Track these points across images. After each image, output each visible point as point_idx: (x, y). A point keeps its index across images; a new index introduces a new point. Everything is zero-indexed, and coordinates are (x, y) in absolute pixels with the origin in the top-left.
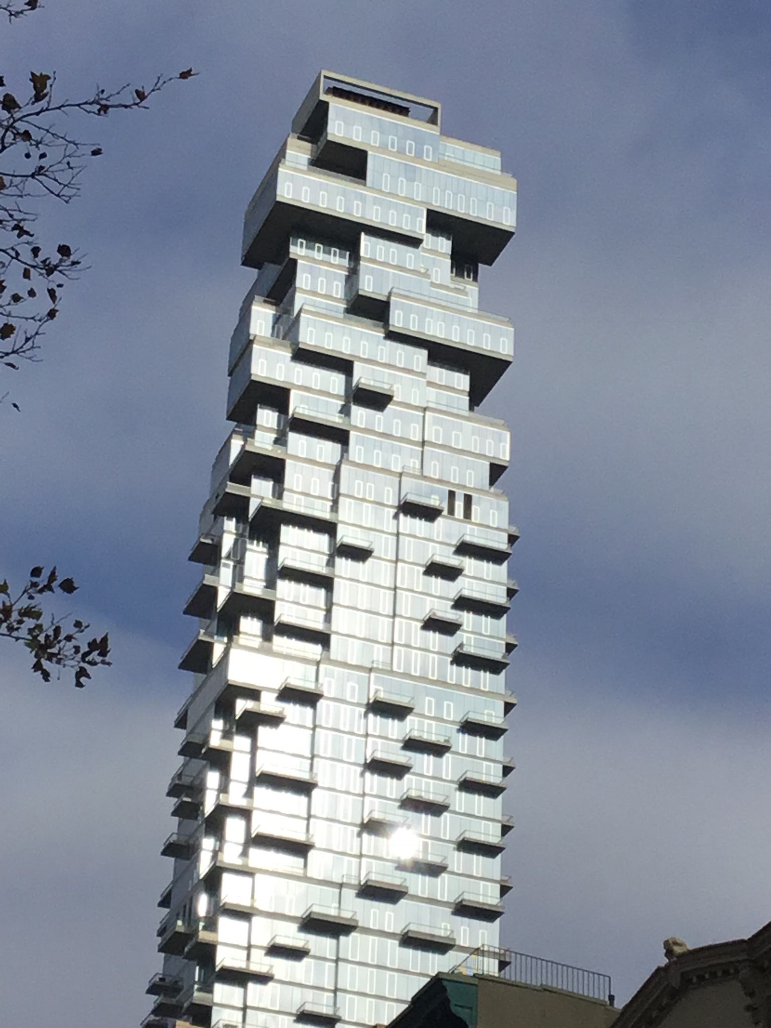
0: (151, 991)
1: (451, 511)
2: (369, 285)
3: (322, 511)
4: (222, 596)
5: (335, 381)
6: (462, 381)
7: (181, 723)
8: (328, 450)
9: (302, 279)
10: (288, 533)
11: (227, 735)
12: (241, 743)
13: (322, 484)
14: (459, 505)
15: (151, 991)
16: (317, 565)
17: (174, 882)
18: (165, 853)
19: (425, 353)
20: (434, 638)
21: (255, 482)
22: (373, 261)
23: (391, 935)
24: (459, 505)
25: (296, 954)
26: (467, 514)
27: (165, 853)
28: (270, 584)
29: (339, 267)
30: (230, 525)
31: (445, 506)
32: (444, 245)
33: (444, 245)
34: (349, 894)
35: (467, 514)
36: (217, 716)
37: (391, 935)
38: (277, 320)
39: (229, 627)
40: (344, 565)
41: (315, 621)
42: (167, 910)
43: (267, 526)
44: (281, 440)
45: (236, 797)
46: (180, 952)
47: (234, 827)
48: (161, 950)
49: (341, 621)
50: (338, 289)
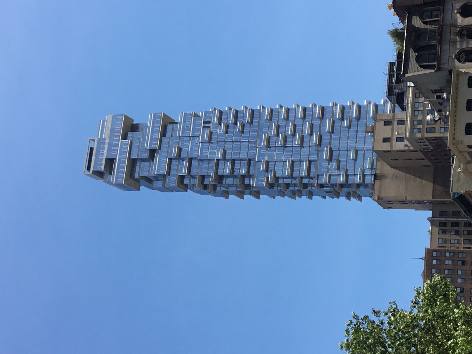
0: (350, 200)
1: (209, 127)
2: (146, 156)
3: (213, 164)
4: (239, 190)
5: (174, 163)
6: (170, 127)
7: (274, 197)
8: (195, 163)
9: (145, 174)
10: (220, 172)
11: (279, 185)
12: (280, 181)
13: (205, 164)
14: (207, 125)
15: (350, 200)
16: (229, 165)
17: (319, 196)
18: (312, 199)
19: (163, 138)
20: (246, 129)
21: (205, 183)
22: (138, 155)
23: (331, 136)
24: (207, 125)
25: (339, 162)
26: (209, 122)
27: (312, 199)
28: (235, 177)
29: (140, 164)
30: (218, 189)
31: (209, 129)
32: (130, 134)
33: (130, 134)
34: (320, 148)
35: (209, 122)
36: (273, 188)
37: (331, 136)
38: (157, 180)
39: (248, 187)
40: (228, 157)
41: (245, 163)
42: (327, 197)
43: (220, 178)
44: (194, 177)
45: (297, 182)
46: (339, 193)
47: (305, 181)
48: (339, 198)
49: (243, 155)
50: (147, 164)
